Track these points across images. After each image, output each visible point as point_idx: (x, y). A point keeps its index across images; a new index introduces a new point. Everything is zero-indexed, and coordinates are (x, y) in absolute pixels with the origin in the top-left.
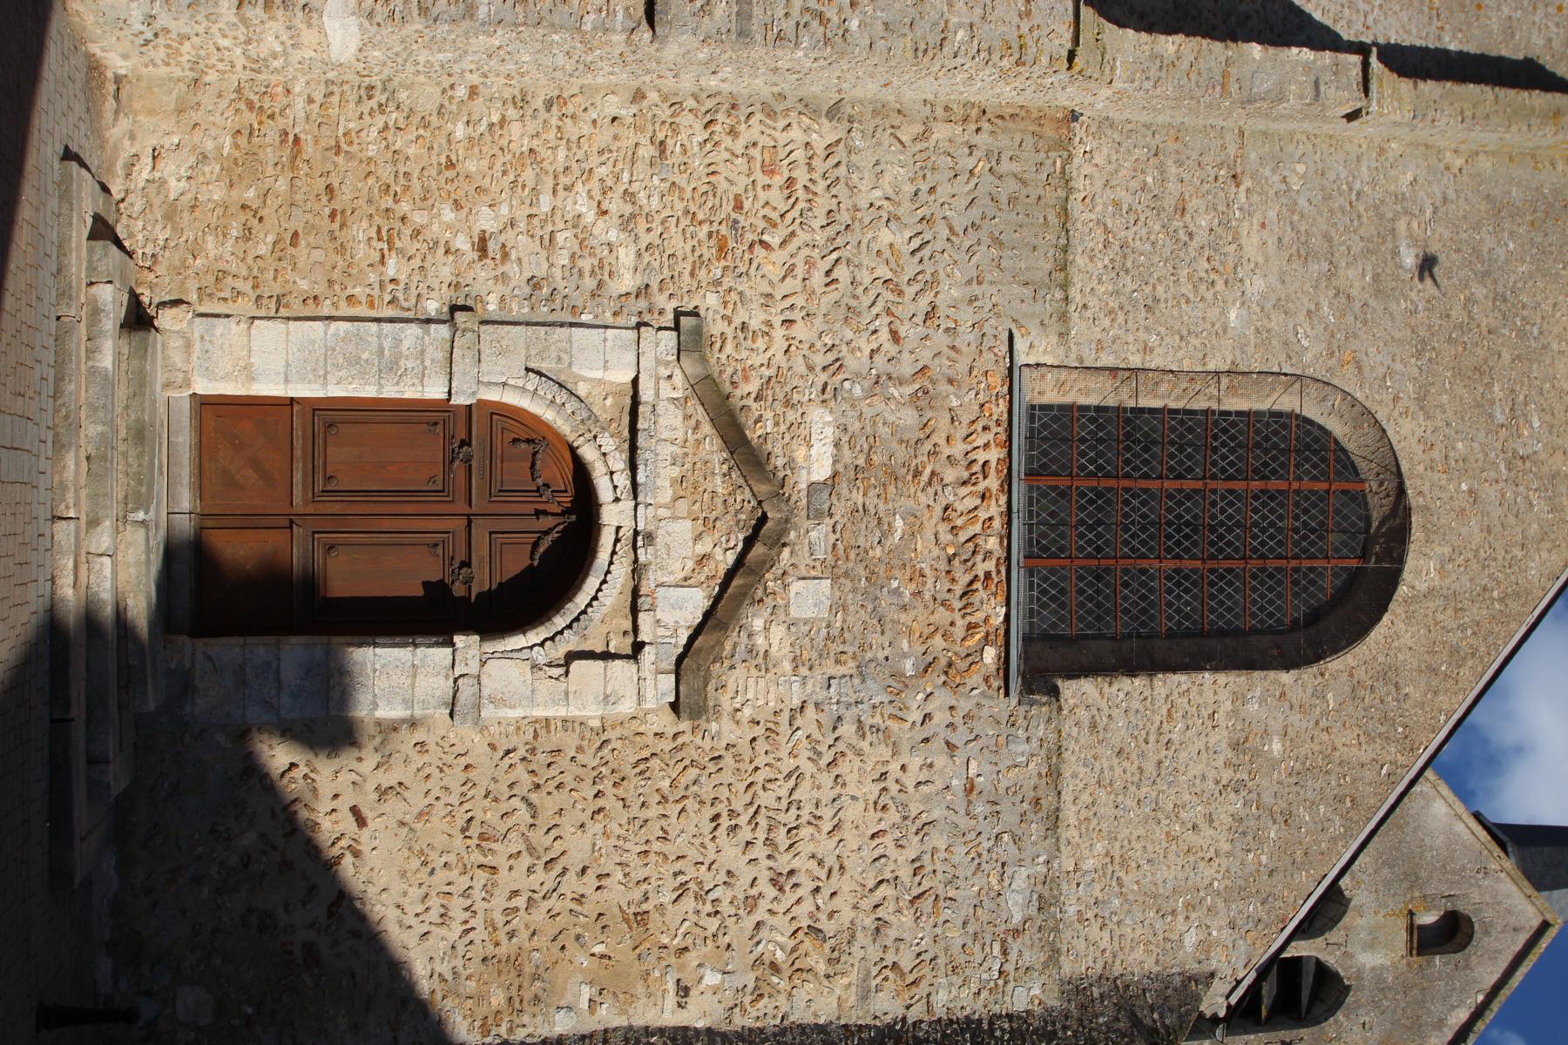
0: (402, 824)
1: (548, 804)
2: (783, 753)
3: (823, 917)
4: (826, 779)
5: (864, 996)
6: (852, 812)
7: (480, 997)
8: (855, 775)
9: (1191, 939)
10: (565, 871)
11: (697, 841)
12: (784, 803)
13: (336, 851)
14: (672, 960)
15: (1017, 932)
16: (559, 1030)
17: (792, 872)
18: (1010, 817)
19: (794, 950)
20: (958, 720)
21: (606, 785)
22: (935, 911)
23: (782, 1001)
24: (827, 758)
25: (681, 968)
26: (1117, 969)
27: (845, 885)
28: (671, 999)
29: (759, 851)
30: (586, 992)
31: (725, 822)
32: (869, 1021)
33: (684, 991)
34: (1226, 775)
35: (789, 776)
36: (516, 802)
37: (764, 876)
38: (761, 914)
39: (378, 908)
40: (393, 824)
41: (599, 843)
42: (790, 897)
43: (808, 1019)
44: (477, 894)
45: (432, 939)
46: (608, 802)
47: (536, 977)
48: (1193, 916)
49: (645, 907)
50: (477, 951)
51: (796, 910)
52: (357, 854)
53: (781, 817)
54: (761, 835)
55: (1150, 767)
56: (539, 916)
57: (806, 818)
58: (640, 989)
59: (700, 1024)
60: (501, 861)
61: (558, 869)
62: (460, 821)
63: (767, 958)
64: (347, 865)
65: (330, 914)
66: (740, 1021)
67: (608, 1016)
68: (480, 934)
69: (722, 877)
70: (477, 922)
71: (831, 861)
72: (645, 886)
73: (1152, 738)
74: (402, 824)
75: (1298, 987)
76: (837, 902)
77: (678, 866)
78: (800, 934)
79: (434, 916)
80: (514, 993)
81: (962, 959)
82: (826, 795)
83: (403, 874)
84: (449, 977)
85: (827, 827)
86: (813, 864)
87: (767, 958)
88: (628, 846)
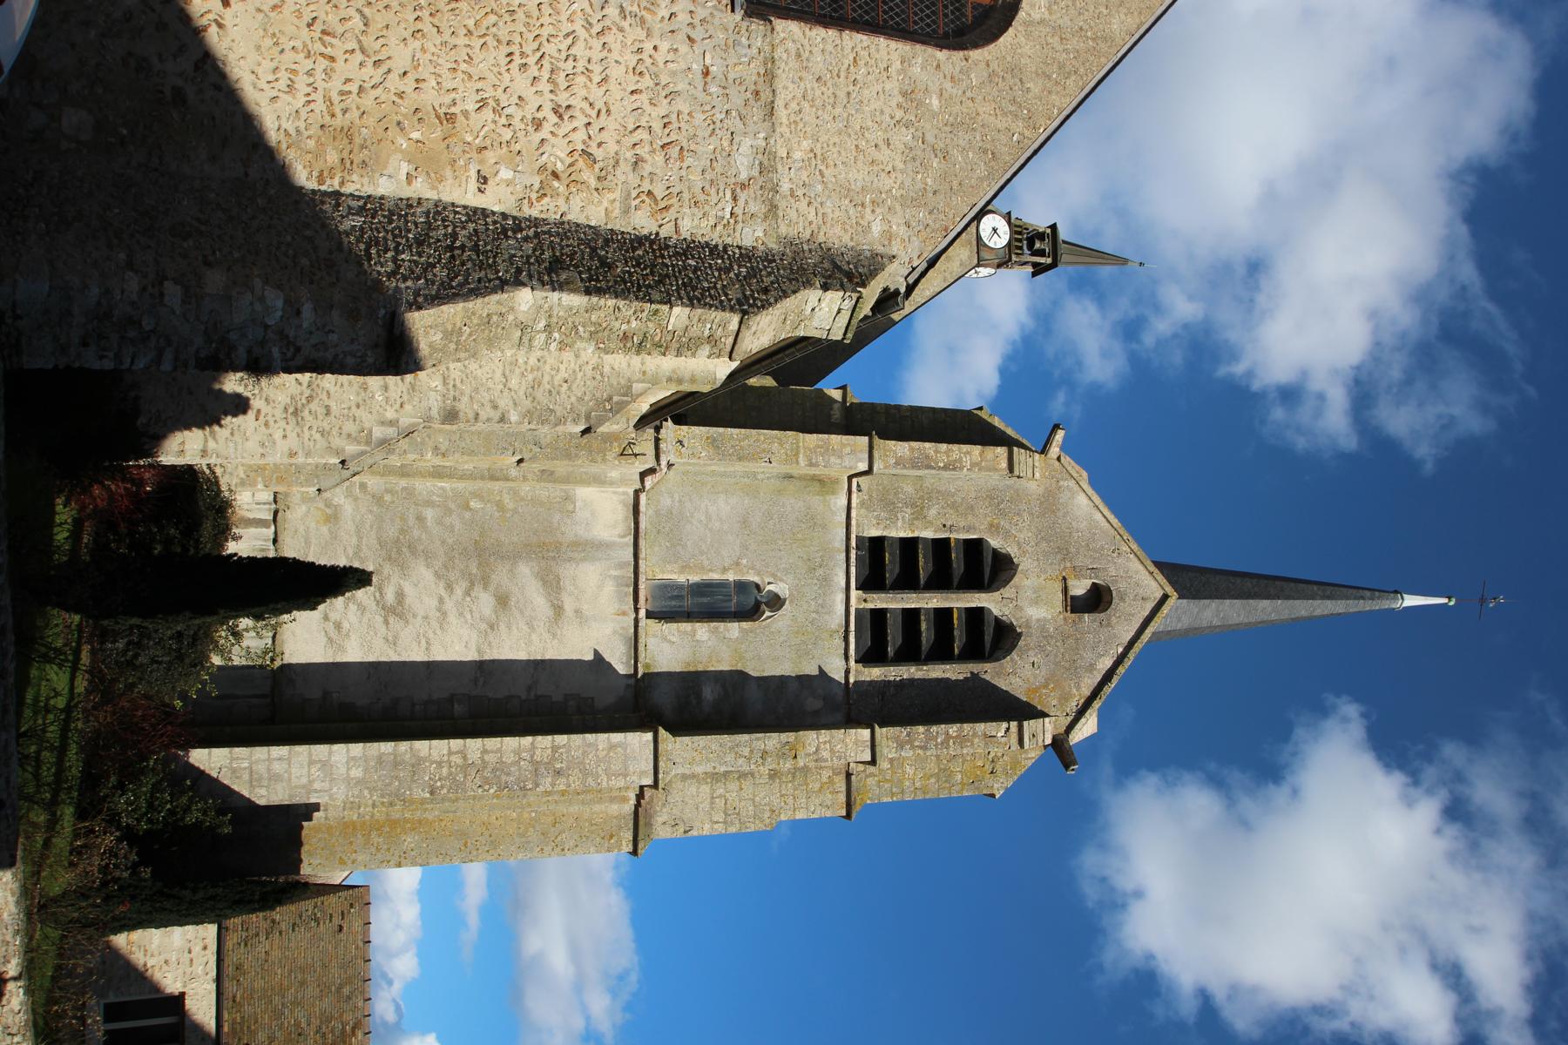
0: (259, 10)
1: (379, 20)
2: (563, 18)
3: (594, 144)
4: (597, 44)
5: (626, 211)
6: (616, 72)
7: (318, 154)
8: (618, 45)
9: (877, 228)
10: (389, 71)
11: (496, 70)
12: (564, 55)
13: (204, 21)
14: (475, 155)
15: (743, 186)
16: (381, 191)
17: (569, 107)
18: (737, 100)
19: (571, 165)
20: (696, 22)
21: (425, 14)
22: (681, 159)
23: (561, 202)
24: (597, 28)
25: (481, 162)
26: (821, 239)
27: (611, 124)
28: (473, 185)
29: (544, 86)
30: (405, 168)
31: (518, 60)
32: (629, 230)
33: (483, 180)
34: (899, 114)
35: (568, 35)
36: (352, 12)
37: (548, 107)
38: (544, 133)
39: (236, 70)
40: (251, 9)
41: (418, 55)
42: (567, 126)
43: (582, 220)
44: (319, 75)
45: (279, 104)
46: (426, 26)
47: (363, 147)
48: (878, 211)
49: (453, 110)
50: (316, 119)
51: (573, 136)
52: (220, 26)
53: (561, 65)
54: (546, 75)
55: (842, 95)
56: (368, 101)
57: (580, 69)
58: (448, 173)
59: (496, 209)
60: (338, 54)
61: (384, 68)
62: (307, 18)
63: (550, 167)
64: (213, 30)
65: (197, 67)
66: (527, 211)
67: (421, 189)
68: (320, 106)
69: (515, 100)
70: (318, 96)
71: (599, 104)
72: (453, 95)
73: (843, 74)
74: (259, 10)
76: (604, 136)
77: (480, 85)
78: (576, 155)
79: (282, 84)
80: (345, 154)
81: (701, 197)
82: (596, 55)
83: (258, 48)
84: (293, 132)
85: (596, 79)
86: (585, 105)
87: (550, 167)
88: (441, 61)
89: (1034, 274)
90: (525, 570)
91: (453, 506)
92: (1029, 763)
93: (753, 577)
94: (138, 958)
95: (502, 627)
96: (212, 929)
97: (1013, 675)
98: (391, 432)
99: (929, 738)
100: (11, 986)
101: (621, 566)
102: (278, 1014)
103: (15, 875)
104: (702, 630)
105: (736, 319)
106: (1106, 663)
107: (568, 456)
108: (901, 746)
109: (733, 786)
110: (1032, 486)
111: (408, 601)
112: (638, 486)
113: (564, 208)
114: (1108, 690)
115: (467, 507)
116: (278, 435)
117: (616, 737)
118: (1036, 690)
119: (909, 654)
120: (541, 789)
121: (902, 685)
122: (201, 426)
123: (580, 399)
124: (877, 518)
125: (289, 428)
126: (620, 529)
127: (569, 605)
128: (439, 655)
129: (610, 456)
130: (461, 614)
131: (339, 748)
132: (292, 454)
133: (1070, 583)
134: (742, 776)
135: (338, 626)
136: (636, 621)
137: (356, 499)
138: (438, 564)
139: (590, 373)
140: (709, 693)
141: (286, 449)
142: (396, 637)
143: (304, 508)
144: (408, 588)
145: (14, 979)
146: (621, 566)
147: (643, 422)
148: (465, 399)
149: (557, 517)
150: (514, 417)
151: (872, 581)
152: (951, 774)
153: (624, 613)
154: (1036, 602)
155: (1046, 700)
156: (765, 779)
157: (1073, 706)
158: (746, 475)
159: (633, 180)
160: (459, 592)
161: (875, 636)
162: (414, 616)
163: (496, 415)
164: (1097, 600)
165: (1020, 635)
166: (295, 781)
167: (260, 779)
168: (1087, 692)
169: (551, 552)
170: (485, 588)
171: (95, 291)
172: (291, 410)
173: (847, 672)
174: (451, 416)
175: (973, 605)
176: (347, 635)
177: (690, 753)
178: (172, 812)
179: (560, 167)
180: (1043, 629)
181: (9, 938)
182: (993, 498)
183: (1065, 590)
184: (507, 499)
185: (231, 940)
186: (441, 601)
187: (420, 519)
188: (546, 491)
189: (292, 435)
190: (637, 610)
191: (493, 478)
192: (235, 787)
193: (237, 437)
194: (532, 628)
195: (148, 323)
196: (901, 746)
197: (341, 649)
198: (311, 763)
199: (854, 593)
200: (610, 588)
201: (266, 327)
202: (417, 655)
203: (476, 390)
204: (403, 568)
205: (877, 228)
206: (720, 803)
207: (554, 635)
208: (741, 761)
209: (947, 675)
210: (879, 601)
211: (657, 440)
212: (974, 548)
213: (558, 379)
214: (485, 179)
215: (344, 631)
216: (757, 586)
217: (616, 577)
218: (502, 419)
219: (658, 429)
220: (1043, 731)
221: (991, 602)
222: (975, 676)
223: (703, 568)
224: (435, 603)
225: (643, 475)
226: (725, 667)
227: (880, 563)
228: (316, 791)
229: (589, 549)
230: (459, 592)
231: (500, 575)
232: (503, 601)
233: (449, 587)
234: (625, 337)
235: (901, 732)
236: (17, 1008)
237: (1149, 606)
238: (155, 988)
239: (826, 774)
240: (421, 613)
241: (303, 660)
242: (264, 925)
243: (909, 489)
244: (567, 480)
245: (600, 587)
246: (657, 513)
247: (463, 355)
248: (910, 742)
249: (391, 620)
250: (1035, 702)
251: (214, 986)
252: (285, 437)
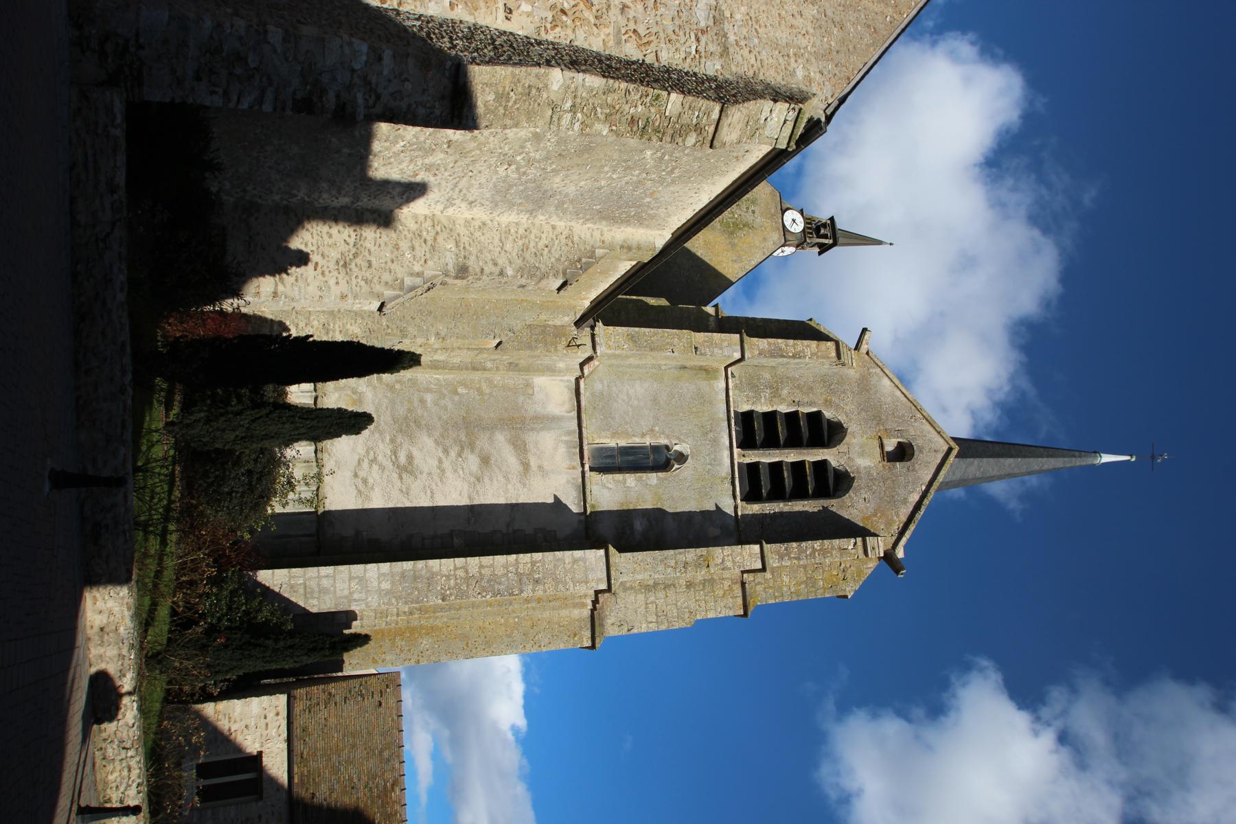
5: (619, 43)
15: (703, 32)
16: (430, 12)
22: (656, 8)
23: (569, 31)
26: (761, 77)
28: (501, 14)
32: (622, 56)
43: (586, 46)
75: (827, 479)
81: (674, 37)
89: (820, 254)
90: (500, 437)
91: (445, 392)
92: (870, 571)
93: (663, 441)
94: (223, 725)
95: (486, 480)
96: (283, 698)
97: (851, 507)
98: (418, 281)
99: (801, 551)
100: (126, 701)
101: (569, 433)
102: (335, 770)
103: (130, 589)
104: (631, 479)
105: (717, 108)
106: (915, 497)
107: (530, 347)
108: (781, 558)
109: (661, 594)
110: (851, 372)
111: (416, 462)
112: (578, 373)
113: (572, 37)
114: (919, 516)
115: (456, 393)
116: (332, 282)
117: (578, 554)
118: (868, 518)
119: (777, 494)
120: (524, 595)
121: (781, 514)
122: (273, 275)
123: (558, 260)
125: (340, 277)
126: (567, 406)
127: (533, 462)
128: (441, 501)
129: (560, 347)
130: (456, 471)
131: (372, 568)
132: (343, 297)
133: (885, 441)
134: (667, 587)
135: (365, 481)
136: (583, 473)
137: (375, 388)
138: (437, 434)
139: (564, 241)
140: (639, 525)
141: (338, 293)
142: (408, 489)
143: (337, 395)
144: (415, 453)
145: (130, 693)
146: (569, 433)
147: (578, 323)
148: (473, 258)
149: (521, 398)
150: (510, 272)
151: (747, 442)
152: (815, 582)
153: (574, 468)
155: (878, 525)
156: (684, 589)
157: (895, 528)
158: (654, 366)
159: (622, 21)
160: (453, 454)
161: (753, 483)
162: (421, 473)
163: (496, 270)
164: (903, 453)
166: (339, 593)
167: (312, 592)
168: (904, 519)
169: (519, 424)
170: (472, 451)
171: (208, 23)
172: (342, 263)
173: (736, 507)
174: (462, 272)
175: (819, 458)
176: (372, 488)
177: (634, 566)
178: (247, 613)
179: (566, 6)
180: (869, 474)
181: (125, 652)
182: (824, 380)
183: (882, 446)
184: (484, 386)
185: (298, 707)
186: (440, 461)
187: (422, 401)
188: (513, 379)
189: (343, 282)
190: (583, 465)
191: (475, 369)
192: (293, 599)
193: (301, 283)
194: (508, 479)
195: (252, 61)
196: (781, 558)
197: (368, 498)
198: (351, 578)
199: (736, 451)
200: (562, 450)
201: (353, 71)
202: (424, 502)
203: (481, 251)
204: (411, 437)
205: (800, 73)
206: (652, 607)
207: (524, 485)
208: (669, 570)
209: (806, 509)
210: (753, 457)
211: (593, 336)
212: (815, 417)
213: (541, 245)
214: (511, 12)
215: (370, 485)
216: (667, 448)
217: (566, 442)
218: (501, 273)
219: (593, 328)
220: (879, 546)
221: (831, 456)
222: (825, 509)
223: (628, 433)
224: (436, 462)
225: (582, 365)
226: (649, 506)
227: (753, 429)
228: (355, 600)
229: (546, 421)
230: (453, 454)
231: (482, 442)
232: (485, 460)
233: (446, 451)
234: (633, 121)
235: (782, 547)
236: (131, 723)
237: (940, 457)
238: (238, 749)
239: (727, 584)
240: (426, 470)
241: (339, 508)
242: (323, 696)
243: (768, 376)
244: (529, 370)
245: (556, 449)
246: (593, 395)
247: (509, 122)
248: (788, 554)
249: (404, 476)
250: (869, 527)
251: (285, 745)
252: (337, 283)
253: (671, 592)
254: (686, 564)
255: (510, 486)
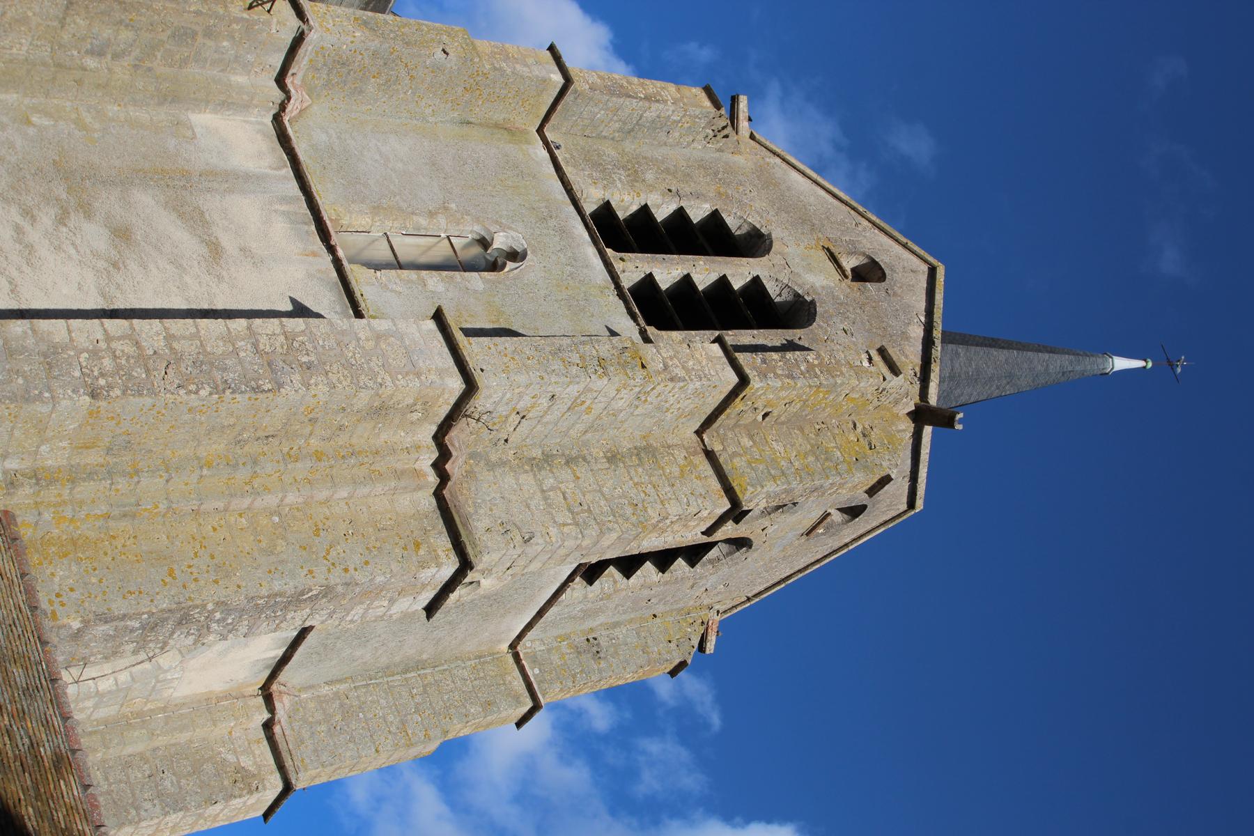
95: (133, 266)
101: (285, 200)
109: (566, 474)
115: (28, 122)
124: (590, 176)
127: (228, 243)
149: (171, 143)
154: (809, 268)
160: (47, 218)
165: (813, 303)
186: (18, 229)
206: (556, 497)
207: (220, 278)
225: (280, 80)
232: (122, 234)
233: (28, 213)
239: (680, 455)
253: (582, 470)
254: (601, 362)
255: (187, 279)
